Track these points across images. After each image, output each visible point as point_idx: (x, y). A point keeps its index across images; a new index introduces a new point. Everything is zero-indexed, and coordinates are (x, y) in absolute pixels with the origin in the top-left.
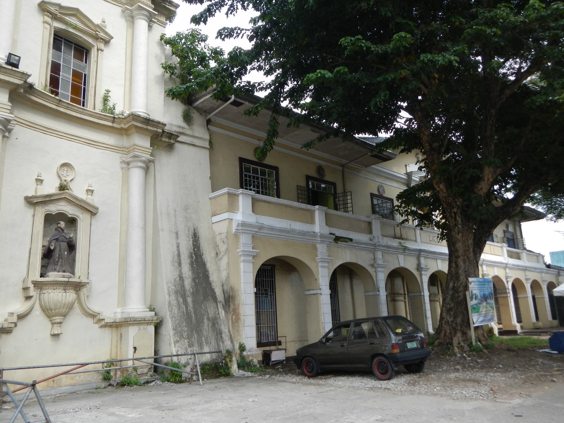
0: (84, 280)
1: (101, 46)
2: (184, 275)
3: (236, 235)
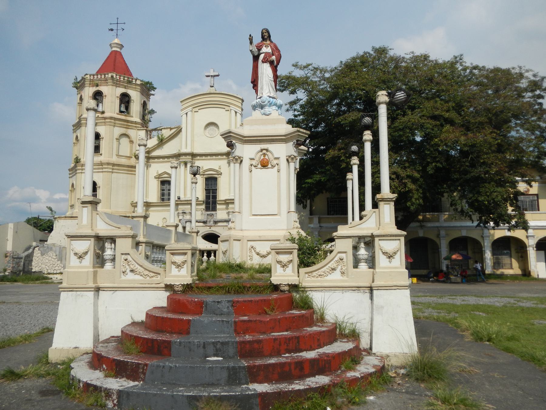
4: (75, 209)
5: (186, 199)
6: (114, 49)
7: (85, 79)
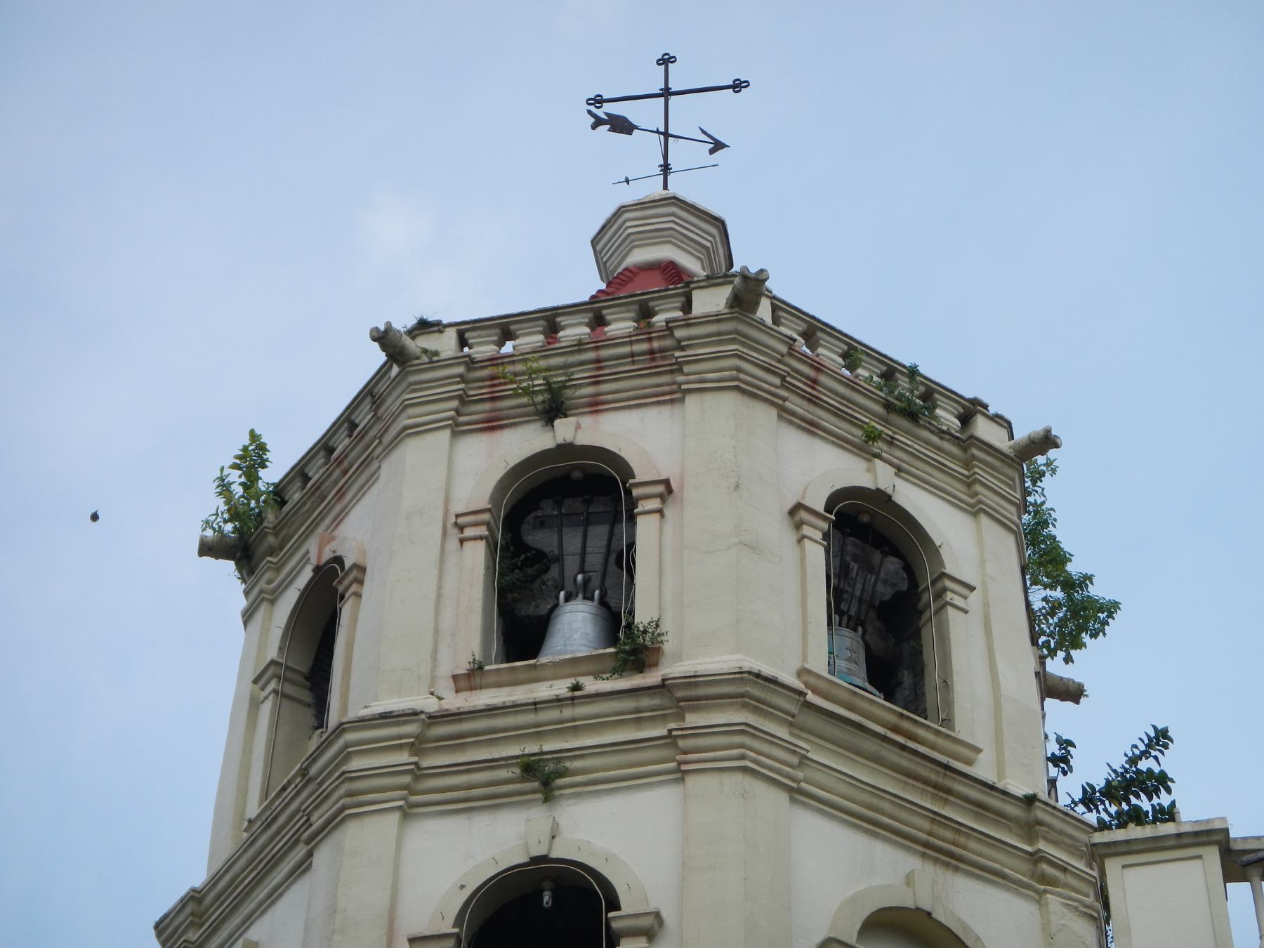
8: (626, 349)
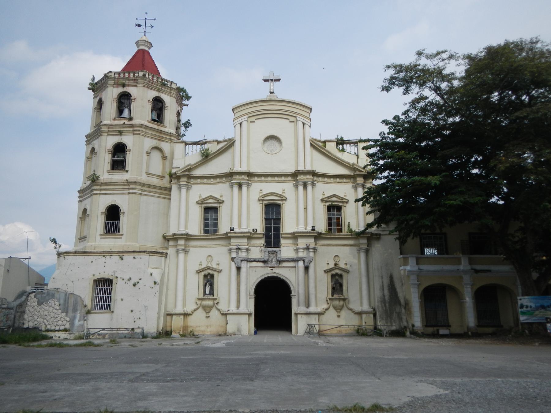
0: (346, 297)
1: (345, 204)
2: (385, 295)
3: (408, 276)
4: (88, 242)
5: (241, 231)
6: (141, 48)
7: (107, 77)
8: (132, 79)
